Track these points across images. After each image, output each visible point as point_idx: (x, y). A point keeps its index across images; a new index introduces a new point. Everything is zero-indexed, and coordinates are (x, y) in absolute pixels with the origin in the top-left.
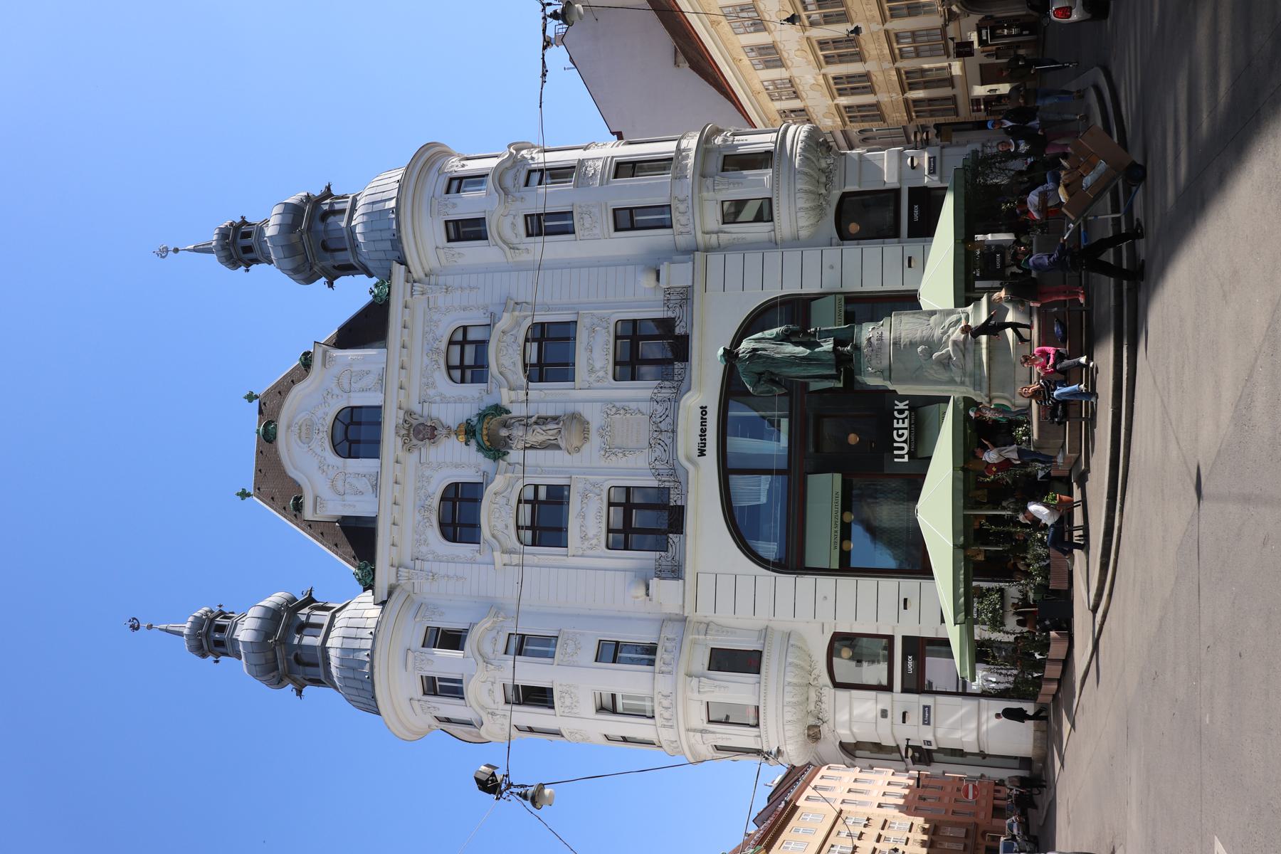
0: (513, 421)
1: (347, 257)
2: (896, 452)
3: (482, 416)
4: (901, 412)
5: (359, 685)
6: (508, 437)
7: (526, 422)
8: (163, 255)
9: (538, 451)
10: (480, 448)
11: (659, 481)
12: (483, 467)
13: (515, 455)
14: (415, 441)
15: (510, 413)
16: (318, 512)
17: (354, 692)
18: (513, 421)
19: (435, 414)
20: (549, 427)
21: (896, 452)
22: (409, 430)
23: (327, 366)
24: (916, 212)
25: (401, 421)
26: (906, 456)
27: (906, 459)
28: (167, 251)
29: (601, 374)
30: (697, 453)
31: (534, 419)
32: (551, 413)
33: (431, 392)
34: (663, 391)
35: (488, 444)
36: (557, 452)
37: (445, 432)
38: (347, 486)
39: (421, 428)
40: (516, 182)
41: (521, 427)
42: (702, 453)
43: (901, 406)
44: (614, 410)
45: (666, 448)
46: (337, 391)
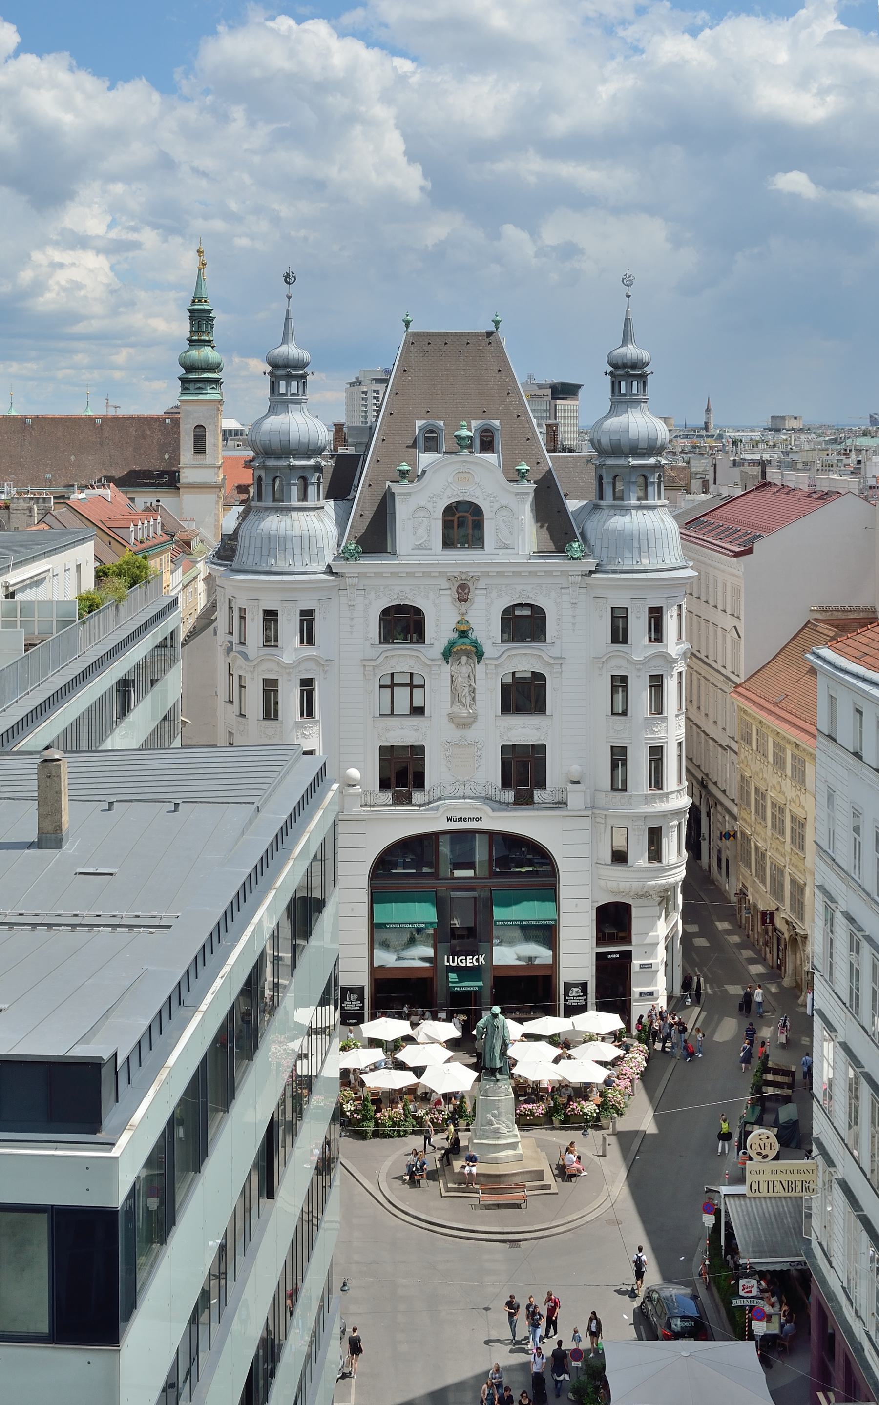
0: (472, 665)
1: (608, 501)
2: (451, 957)
3: (475, 644)
4: (477, 960)
5: (265, 552)
6: (460, 662)
7: (472, 676)
8: (625, 281)
9: (449, 688)
10: (452, 644)
11: (430, 790)
12: (436, 643)
13: (446, 669)
14: (457, 584)
15: (479, 662)
16: (399, 497)
17: (258, 545)
18: (472, 665)
19: (477, 599)
20: (468, 698)
21: (451, 957)
22: (466, 580)
23: (518, 497)
24: (614, 956)
25: (472, 574)
26: (448, 964)
27: (446, 963)
28: (628, 285)
29: (506, 738)
30: (449, 816)
31: (473, 684)
32: (477, 698)
33: (494, 594)
34: (493, 790)
35: (455, 650)
36: (449, 704)
37: (463, 611)
38: (420, 520)
39: (467, 591)
40: (653, 668)
41: (467, 675)
42: (449, 819)
43: (481, 959)
44: (480, 746)
45: (452, 794)
46: (497, 506)
